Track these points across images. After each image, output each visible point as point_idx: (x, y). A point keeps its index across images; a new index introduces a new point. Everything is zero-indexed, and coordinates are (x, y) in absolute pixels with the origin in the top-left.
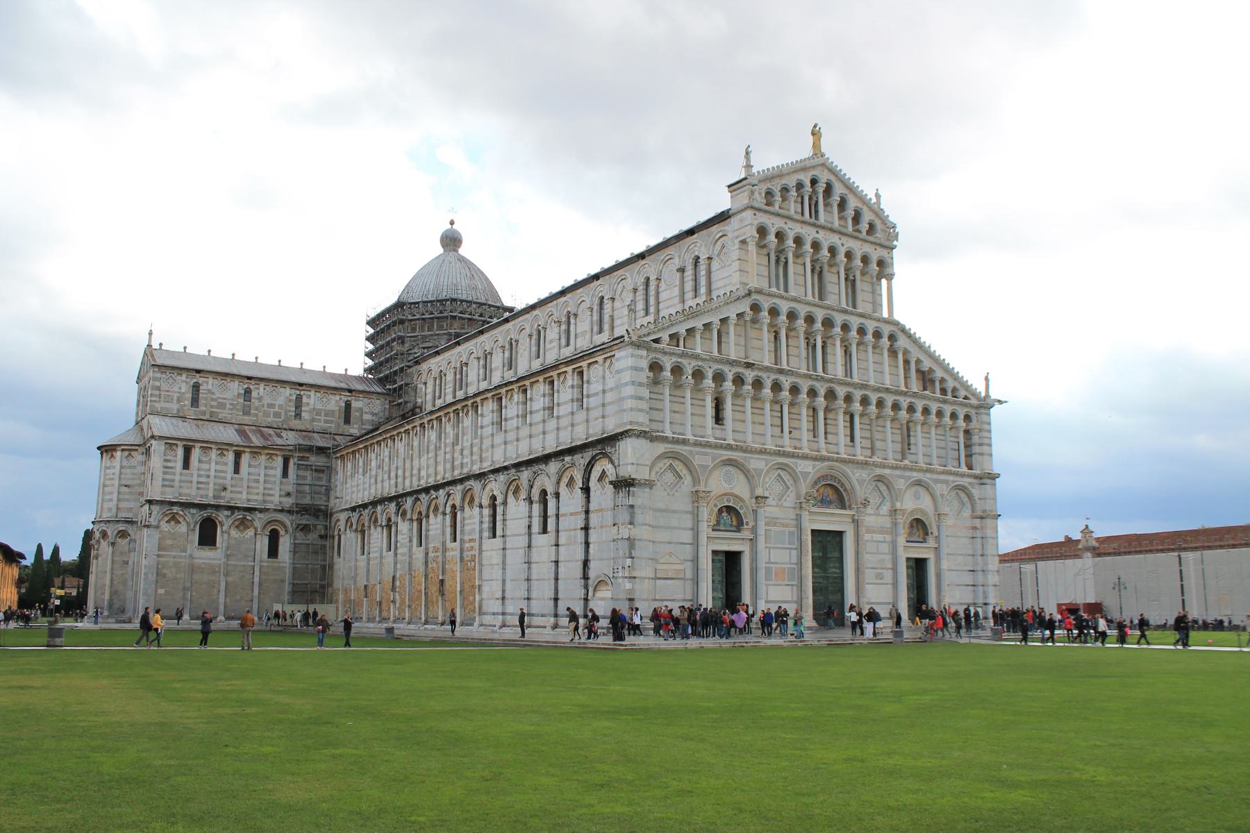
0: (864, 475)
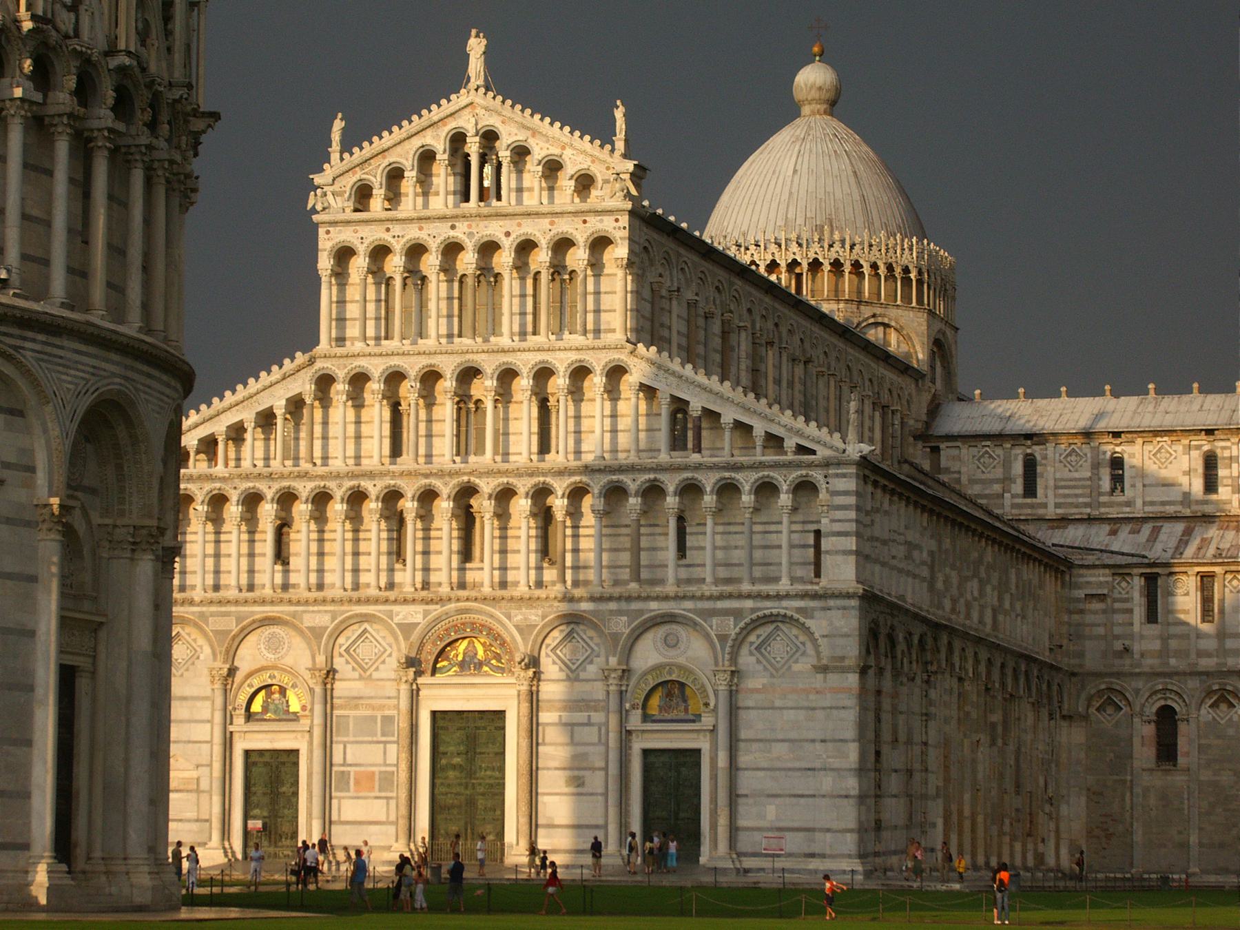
0: (533, 618)
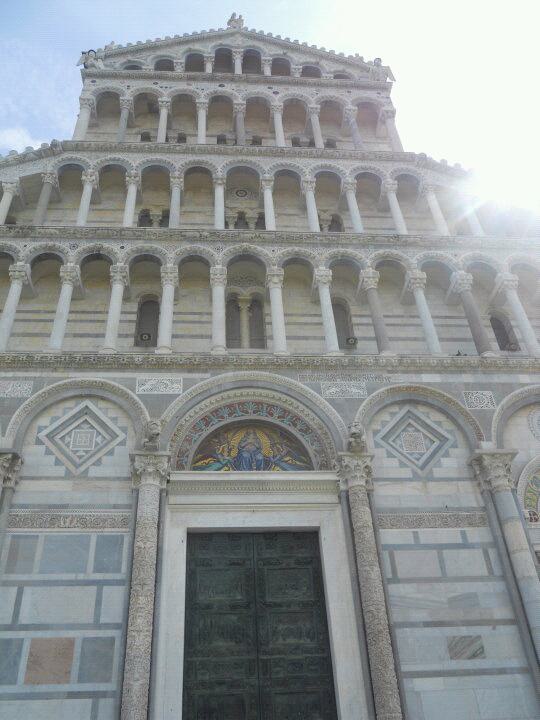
0: (354, 390)
